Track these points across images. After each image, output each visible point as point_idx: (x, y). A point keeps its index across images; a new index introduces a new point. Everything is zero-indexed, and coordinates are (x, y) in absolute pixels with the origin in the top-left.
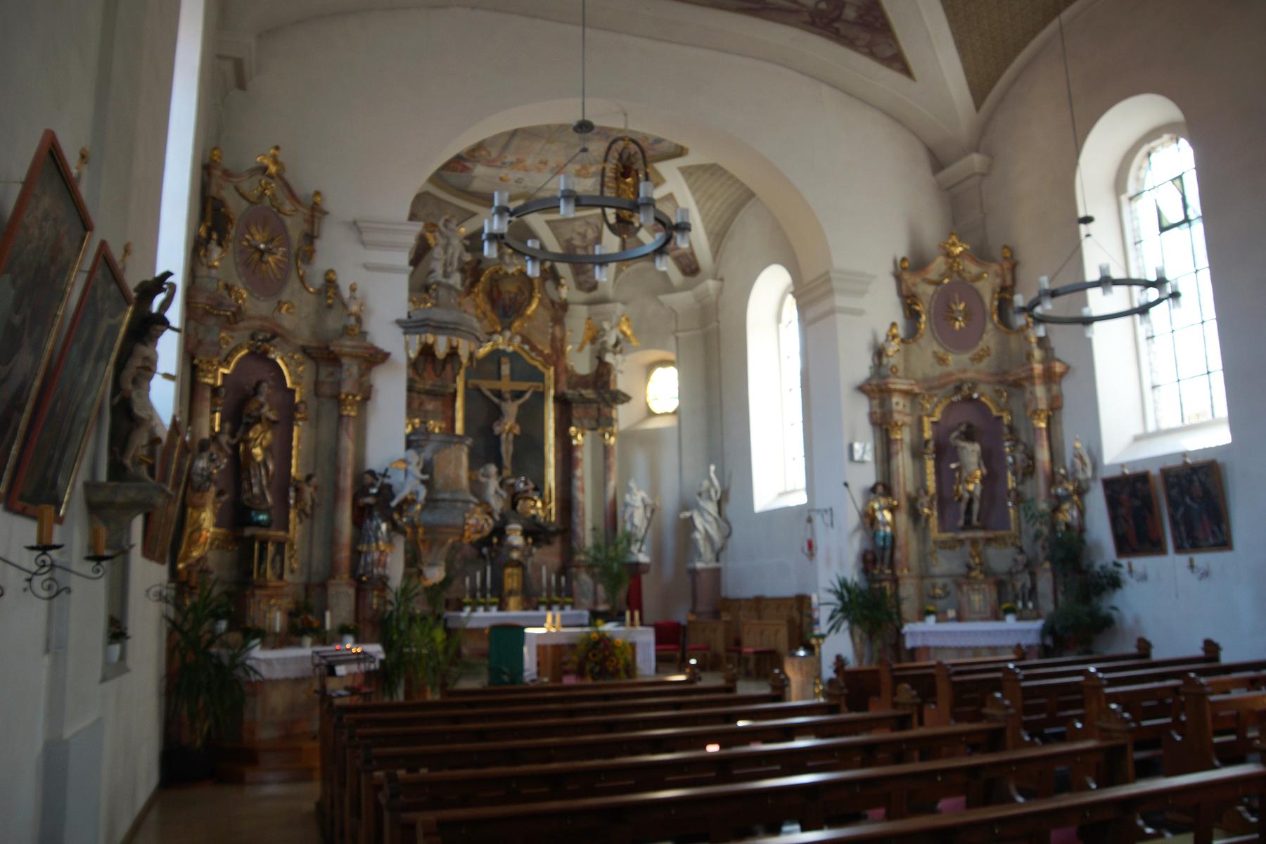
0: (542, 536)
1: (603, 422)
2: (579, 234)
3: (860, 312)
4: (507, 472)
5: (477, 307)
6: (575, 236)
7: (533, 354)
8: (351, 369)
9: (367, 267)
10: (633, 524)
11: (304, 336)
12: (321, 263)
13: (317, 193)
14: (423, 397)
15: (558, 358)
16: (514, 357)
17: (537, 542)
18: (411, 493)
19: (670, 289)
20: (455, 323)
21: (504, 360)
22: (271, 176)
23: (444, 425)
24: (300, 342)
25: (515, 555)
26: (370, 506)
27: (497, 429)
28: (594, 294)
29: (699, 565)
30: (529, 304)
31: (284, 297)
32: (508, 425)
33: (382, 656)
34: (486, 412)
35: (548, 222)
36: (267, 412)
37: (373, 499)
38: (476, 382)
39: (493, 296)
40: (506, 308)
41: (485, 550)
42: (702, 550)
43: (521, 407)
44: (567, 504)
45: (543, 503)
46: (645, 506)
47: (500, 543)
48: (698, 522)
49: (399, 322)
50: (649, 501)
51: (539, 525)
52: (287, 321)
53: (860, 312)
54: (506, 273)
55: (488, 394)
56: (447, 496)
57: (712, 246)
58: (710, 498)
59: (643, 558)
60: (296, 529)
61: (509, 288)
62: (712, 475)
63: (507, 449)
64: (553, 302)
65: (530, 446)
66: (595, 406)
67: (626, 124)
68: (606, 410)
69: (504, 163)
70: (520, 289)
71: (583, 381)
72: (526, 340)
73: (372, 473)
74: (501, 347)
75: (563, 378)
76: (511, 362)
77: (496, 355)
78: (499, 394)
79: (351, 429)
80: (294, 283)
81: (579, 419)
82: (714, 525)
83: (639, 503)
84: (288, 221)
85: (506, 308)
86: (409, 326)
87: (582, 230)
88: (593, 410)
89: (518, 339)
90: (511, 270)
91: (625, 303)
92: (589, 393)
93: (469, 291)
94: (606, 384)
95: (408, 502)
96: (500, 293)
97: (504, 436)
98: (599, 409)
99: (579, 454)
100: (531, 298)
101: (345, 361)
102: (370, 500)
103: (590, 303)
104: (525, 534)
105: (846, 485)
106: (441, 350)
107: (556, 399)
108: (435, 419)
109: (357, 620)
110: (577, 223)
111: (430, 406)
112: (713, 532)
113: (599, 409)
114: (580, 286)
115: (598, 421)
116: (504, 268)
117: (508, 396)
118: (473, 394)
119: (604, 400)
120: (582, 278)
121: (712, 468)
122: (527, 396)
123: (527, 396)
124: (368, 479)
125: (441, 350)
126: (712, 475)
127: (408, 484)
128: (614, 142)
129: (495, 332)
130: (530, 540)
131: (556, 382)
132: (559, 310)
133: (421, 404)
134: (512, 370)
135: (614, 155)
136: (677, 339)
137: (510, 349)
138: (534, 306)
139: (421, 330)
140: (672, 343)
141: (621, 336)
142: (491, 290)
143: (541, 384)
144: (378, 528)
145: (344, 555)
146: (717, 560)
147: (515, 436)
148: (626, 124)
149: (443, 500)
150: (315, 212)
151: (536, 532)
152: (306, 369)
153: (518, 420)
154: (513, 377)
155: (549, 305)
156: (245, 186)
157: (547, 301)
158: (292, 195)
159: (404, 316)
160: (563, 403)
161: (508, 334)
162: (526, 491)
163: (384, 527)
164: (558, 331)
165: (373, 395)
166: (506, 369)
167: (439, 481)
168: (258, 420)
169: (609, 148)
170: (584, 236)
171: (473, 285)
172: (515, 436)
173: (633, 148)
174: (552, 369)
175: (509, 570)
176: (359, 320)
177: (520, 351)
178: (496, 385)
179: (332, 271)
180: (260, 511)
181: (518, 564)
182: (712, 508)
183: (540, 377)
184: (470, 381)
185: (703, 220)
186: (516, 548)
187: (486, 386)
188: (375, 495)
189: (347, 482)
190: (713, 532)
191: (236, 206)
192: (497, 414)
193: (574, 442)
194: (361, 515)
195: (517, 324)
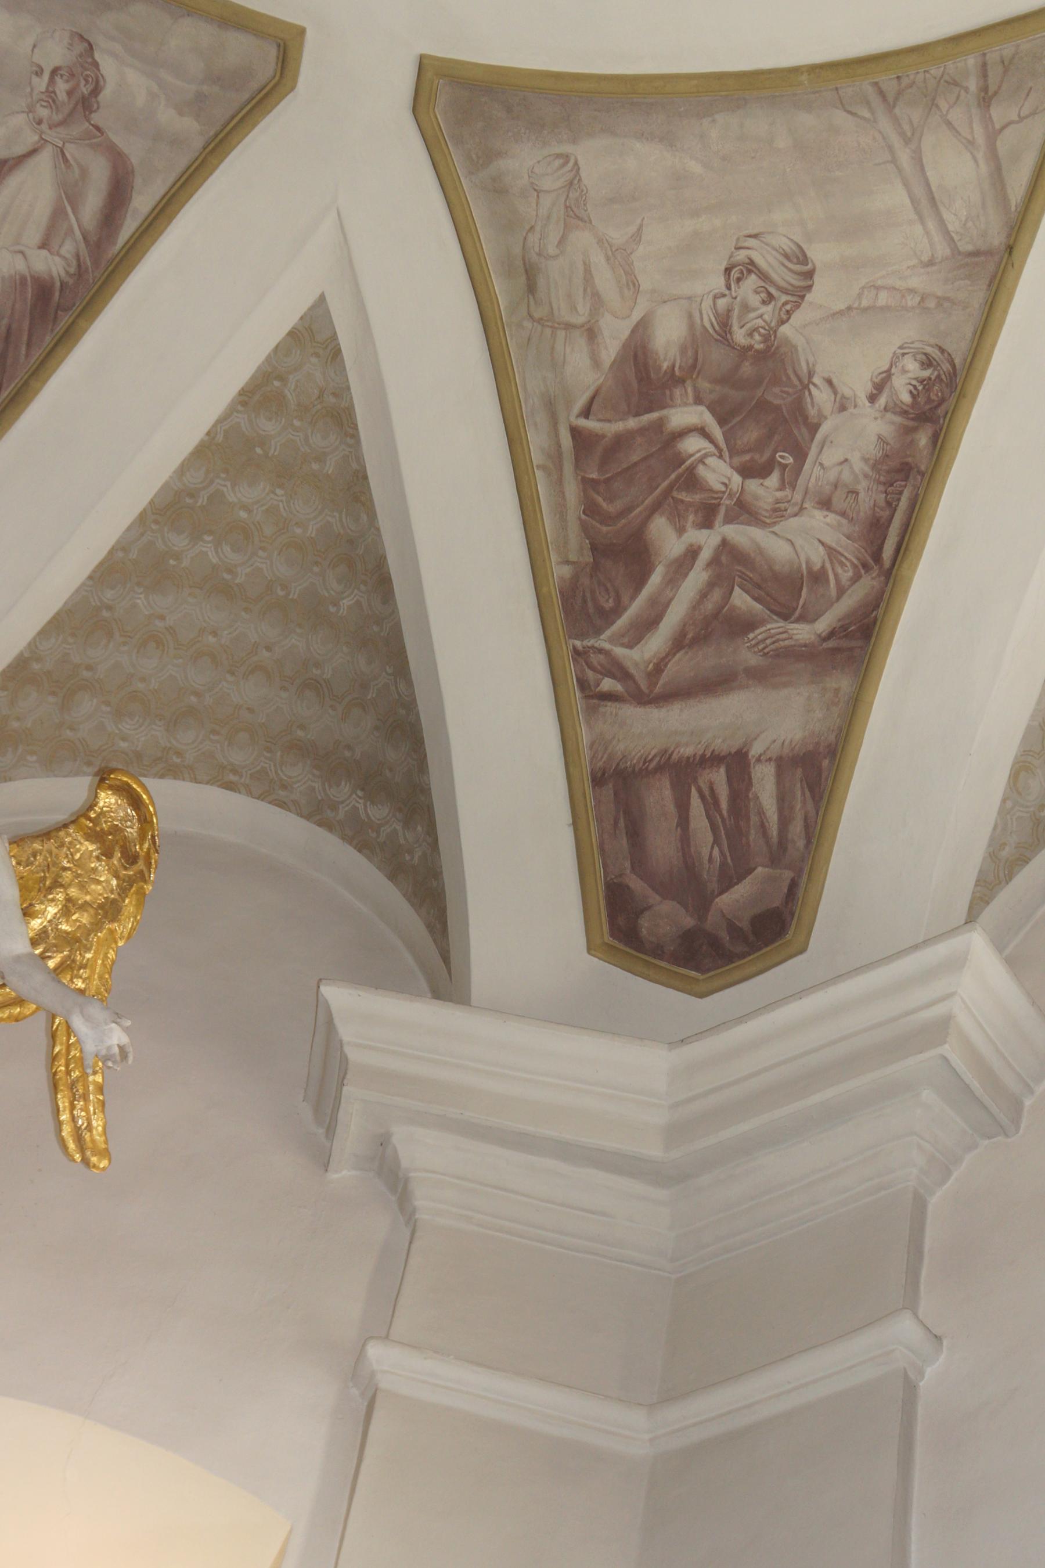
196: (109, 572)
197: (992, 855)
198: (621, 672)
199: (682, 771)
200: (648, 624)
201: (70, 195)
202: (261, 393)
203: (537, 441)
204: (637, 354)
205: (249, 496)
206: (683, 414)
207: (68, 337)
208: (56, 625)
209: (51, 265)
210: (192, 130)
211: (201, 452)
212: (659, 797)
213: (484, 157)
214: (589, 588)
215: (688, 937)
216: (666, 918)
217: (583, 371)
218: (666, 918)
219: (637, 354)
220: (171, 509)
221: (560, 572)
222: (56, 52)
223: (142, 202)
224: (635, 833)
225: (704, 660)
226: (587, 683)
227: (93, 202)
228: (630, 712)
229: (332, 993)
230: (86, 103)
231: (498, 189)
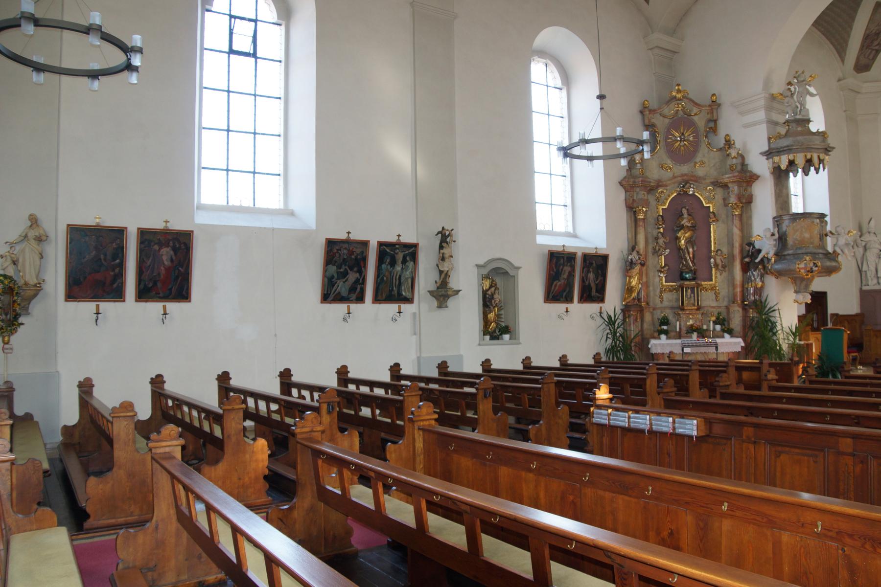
8: (735, 188)
11: (714, 173)
12: (722, 132)
13: (714, 95)
20: (788, 146)
22: (680, 100)
24: (708, 181)
26: (748, 263)
31: (698, 160)
33: (743, 345)
36: (685, 222)
37: (751, 259)
49: (761, 153)
52: (700, 172)
56: (790, 252)
60: (718, 278)
79: (737, 222)
80: (703, 149)
84: (696, 118)
86: (769, 154)
101: (730, 185)
102: (747, 260)
109: (744, 327)
127: (767, 247)
145: (738, 290)
149: (789, 255)
150: (715, 105)
152: (719, 193)
156: (666, 111)
158: (696, 104)
167: (790, 242)
168: (682, 227)
176: (743, 158)
179: (727, 135)
180: (688, 273)
189: (737, 251)
191: (661, 123)
194: (746, 268)
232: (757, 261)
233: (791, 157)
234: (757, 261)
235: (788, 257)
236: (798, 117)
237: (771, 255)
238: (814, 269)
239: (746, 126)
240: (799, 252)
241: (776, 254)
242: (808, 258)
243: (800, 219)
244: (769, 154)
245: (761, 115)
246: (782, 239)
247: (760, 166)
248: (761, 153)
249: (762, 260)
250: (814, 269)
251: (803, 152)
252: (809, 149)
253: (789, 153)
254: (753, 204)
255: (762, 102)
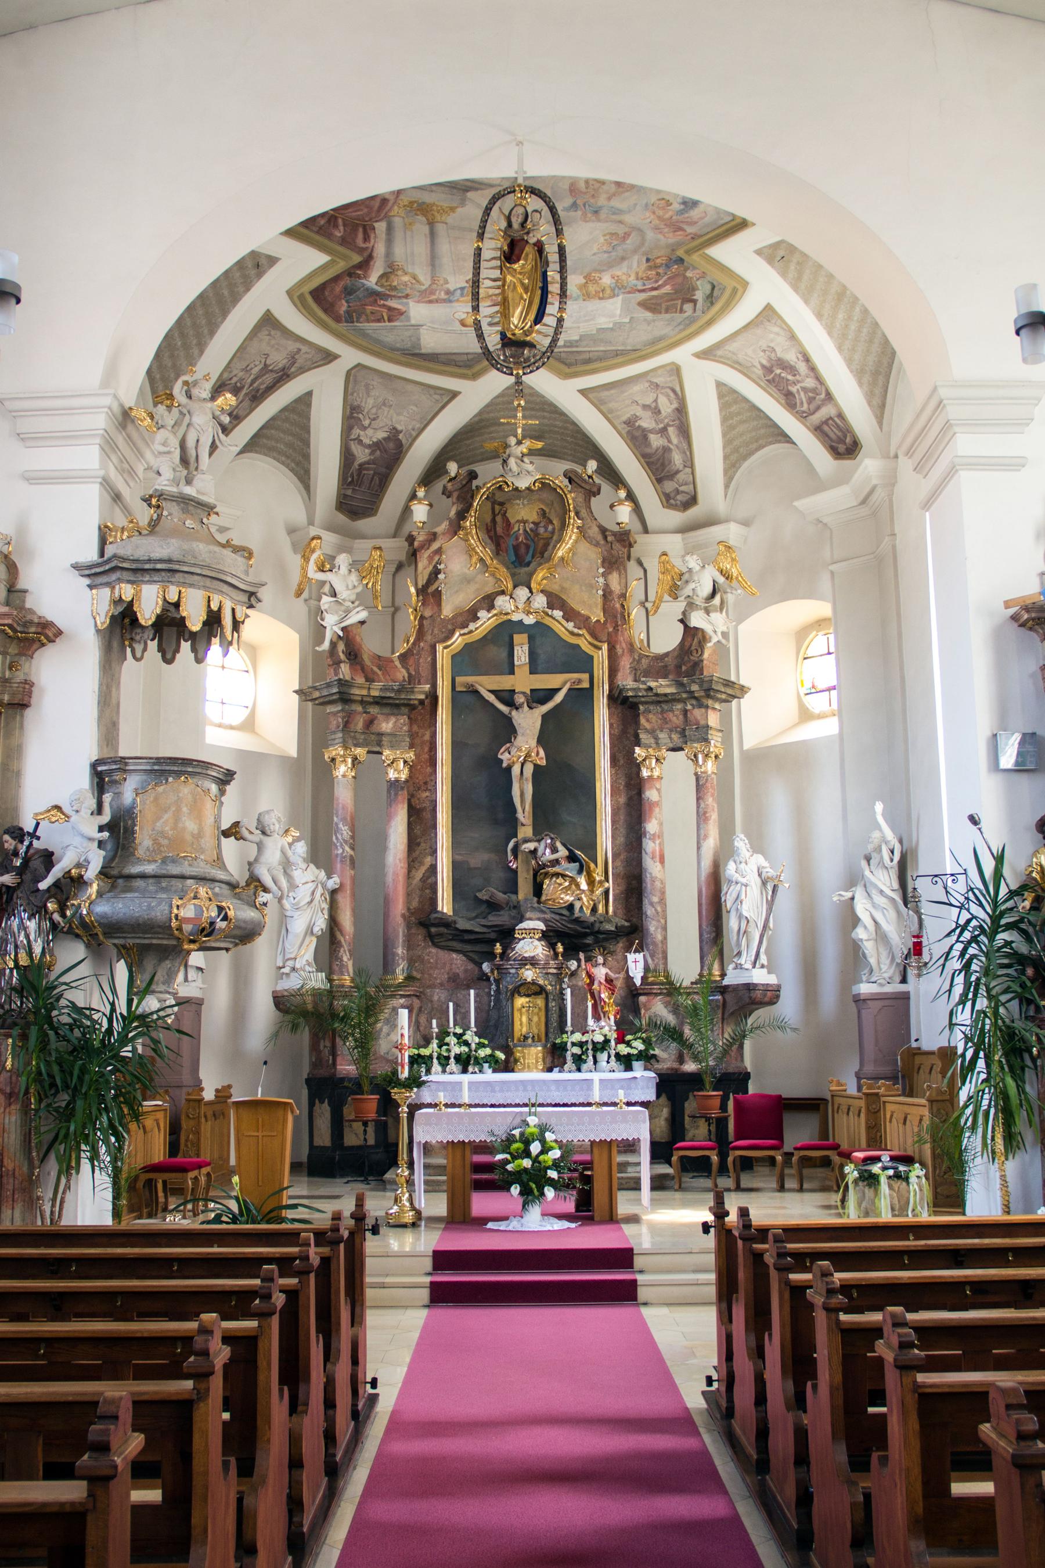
0: (589, 940)
1: (690, 736)
2: (645, 407)
3: (1016, 464)
4: (526, 831)
5: (470, 551)
6: (640, 412)
7: (570, 625)
9: (32, 478)
10: (740, 917)
14: (374, 710)
15: (616, 627)
16: (538, 633)
17: (571, 952)
18: (78, 865)
19: (816, 484)
20: (169, 561)
21: (518, 638)
23: (411, 755)
25: (529, 974)
27: (504, 757)
28: (693, 512)
29: (865, 989)
30: (560, 540)
32: (525, 749)
34: (487, 726)
35: (583, 392)
38: (470, 679)
39: (497, 533)
40: (522, 552)
41: (486, 967)
42: (872, 961)
43: (545, 717)
44: (634, 886)
45: (591, 882)
46: (764, 883)
47: (503, 955)
48: (862, 908)
49: (76, 567)
50: (771, 873)
51: (577, 921)
53: (1016, 464)
54: (516, 489)
55: (491, 698)
56: (150, 868)
57: (869, 396)
58: (881, 864)
59: (760, 977)
61: (523, 514)
62: (880, 819)
63: (523, 792)
64: (603, 531)
65: (563, 788)
66: (679, 706)
67: (521, 161)
68: (698, 713)
69: (448, 292)
70: (543, 514)
71: (659, 666)
72: (555, 601)
73: (19, 834)
74: (515, 617)
75: (625, 663)
76: (531, 639)
77: (505, 632)
78: (507, 697)
81: (652, 732)
82: (892, 914)
83: (755, 882)
85: (522, 552)
86: (101, 571)
87: (649, 400)
88: (676, 718)
89: (540, 601)
90: (523, 483)
91: (746, 523)
92: (664, 686)
93: (456, 527)
94: (697, 666)
95: (73, 883)
96: (508, 525)
97: (516, 770)
98: (685, 712)
99: (651, 794)
100: (563, 526)
103: (685, 529)
104: (549, 937)
105: (974, 820)
106: (148, 611)
107: (611, 698)
108: (392, 747)
110: (637, 388)
111: (387, 725)
112: (890, 927)
113: (685, 712)
114: (668, 500)
115: (683, 733)
116: (510, 480)
117: (520, 699)
118: (466, 700)
119: (692, 695)
120: (669, 486)
121: (879, 807)
122: (559, 698)
123: (559, 698)
124: (9, 843)
125: (149, 604)
126: (880, 819)
127: (77, 845)
128: (494, 200)
129: (503, 593)
130: (560, 948)
131: (613, 671)
132: (617, 548)
133: (370, 723)
134: (532, 654)
135: (497, 223)
136: (832, 573)
137: (530, 620)
138: (571, 536)
139: (114, 577)
140: (825, 584)
141: (721, 580)
142: (494, 521)
143: (585, 676)
144: (23, 927)
146: (904, 980)
147: (536, 765)
148: (521, 161)
149: (143, 876)
151: (573, 937)
153: (540, 741)
154: (534, 668)
155: (600, 537)
157: (594, 532)
159: (91, 555)
160: (625, 705)
161: (522, 593)
162: (556, 862)
163: (32, 925)
164: (614, 580)
165: (34, 701)
166: (522, 655)
167: (143, 840)
169: (487, 211)
170: (657, 411)
171: (462, 515)
172: (536, 765)
173: (534, 203)
174: (605, 647)
175: (520, 1001)
177: (548, 621)
178: (504, 682)
181: (536, 990)
182: (885, 880)
183: (585, 663)
184: (459, 680)
185: (840, 349)
186: (533, 962)
187: (486, 684)
188: (21, 871)
190: (890, 927)
192: (507, 731)
193: (645, 773)
195: (540, 575)
196: (724, 435)
197: (876, 417)
198: (804, 412)
199: (826, 422)
200: (802, 403)
201: (668, 396)
202: (720, 396)
203: (762, 384)
204: (763, 366)
205: (734, 408)
206: (778, 371)
207: (686, 413)
208: (724, 448)
209: (675, 405)
210: (674, 377)
211: (721, 410)
212: (826, 428)
213: (715, 356)
214: (789, 401)
215: (847, 449)
216: (842, 448)
217: (760, 372)
218: (842, 448)
219: (763, 366)
220: (724, 420)
221: (783, 402)
222: (647, 385)
223: (678, 389)
224: (827, 436)
225: (812, 407)
226: (803, 417)
227: (672, 395)
228: (811, 417)
229: (796, 504)
230: (657, 385)
231: (721, 357)
232: (43, 885)
233: (173, 597)
234: (43, 885)
235: (139, 883)
236: (189, 490)
237: (91, 873)
238: (221, 925)
239: (32, 478)
240: (175, 870)
241: (104, 873)
242: (202, 891)
243: (178, 774)
244: (101, 571)
245: (88, 457)
246: (119, 831)
247: (70, 604)
248: (76, 567)
249: (57, 884)
250: (221, 925)
251: (205, 588)
252: (216, 579)
253: (165, 583)
254: (28, 713)
255: (100, 421)
